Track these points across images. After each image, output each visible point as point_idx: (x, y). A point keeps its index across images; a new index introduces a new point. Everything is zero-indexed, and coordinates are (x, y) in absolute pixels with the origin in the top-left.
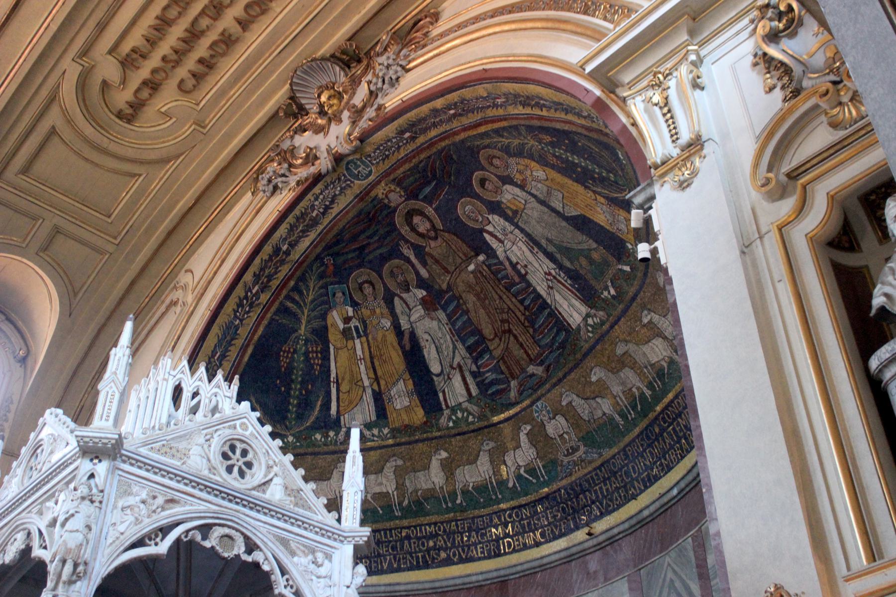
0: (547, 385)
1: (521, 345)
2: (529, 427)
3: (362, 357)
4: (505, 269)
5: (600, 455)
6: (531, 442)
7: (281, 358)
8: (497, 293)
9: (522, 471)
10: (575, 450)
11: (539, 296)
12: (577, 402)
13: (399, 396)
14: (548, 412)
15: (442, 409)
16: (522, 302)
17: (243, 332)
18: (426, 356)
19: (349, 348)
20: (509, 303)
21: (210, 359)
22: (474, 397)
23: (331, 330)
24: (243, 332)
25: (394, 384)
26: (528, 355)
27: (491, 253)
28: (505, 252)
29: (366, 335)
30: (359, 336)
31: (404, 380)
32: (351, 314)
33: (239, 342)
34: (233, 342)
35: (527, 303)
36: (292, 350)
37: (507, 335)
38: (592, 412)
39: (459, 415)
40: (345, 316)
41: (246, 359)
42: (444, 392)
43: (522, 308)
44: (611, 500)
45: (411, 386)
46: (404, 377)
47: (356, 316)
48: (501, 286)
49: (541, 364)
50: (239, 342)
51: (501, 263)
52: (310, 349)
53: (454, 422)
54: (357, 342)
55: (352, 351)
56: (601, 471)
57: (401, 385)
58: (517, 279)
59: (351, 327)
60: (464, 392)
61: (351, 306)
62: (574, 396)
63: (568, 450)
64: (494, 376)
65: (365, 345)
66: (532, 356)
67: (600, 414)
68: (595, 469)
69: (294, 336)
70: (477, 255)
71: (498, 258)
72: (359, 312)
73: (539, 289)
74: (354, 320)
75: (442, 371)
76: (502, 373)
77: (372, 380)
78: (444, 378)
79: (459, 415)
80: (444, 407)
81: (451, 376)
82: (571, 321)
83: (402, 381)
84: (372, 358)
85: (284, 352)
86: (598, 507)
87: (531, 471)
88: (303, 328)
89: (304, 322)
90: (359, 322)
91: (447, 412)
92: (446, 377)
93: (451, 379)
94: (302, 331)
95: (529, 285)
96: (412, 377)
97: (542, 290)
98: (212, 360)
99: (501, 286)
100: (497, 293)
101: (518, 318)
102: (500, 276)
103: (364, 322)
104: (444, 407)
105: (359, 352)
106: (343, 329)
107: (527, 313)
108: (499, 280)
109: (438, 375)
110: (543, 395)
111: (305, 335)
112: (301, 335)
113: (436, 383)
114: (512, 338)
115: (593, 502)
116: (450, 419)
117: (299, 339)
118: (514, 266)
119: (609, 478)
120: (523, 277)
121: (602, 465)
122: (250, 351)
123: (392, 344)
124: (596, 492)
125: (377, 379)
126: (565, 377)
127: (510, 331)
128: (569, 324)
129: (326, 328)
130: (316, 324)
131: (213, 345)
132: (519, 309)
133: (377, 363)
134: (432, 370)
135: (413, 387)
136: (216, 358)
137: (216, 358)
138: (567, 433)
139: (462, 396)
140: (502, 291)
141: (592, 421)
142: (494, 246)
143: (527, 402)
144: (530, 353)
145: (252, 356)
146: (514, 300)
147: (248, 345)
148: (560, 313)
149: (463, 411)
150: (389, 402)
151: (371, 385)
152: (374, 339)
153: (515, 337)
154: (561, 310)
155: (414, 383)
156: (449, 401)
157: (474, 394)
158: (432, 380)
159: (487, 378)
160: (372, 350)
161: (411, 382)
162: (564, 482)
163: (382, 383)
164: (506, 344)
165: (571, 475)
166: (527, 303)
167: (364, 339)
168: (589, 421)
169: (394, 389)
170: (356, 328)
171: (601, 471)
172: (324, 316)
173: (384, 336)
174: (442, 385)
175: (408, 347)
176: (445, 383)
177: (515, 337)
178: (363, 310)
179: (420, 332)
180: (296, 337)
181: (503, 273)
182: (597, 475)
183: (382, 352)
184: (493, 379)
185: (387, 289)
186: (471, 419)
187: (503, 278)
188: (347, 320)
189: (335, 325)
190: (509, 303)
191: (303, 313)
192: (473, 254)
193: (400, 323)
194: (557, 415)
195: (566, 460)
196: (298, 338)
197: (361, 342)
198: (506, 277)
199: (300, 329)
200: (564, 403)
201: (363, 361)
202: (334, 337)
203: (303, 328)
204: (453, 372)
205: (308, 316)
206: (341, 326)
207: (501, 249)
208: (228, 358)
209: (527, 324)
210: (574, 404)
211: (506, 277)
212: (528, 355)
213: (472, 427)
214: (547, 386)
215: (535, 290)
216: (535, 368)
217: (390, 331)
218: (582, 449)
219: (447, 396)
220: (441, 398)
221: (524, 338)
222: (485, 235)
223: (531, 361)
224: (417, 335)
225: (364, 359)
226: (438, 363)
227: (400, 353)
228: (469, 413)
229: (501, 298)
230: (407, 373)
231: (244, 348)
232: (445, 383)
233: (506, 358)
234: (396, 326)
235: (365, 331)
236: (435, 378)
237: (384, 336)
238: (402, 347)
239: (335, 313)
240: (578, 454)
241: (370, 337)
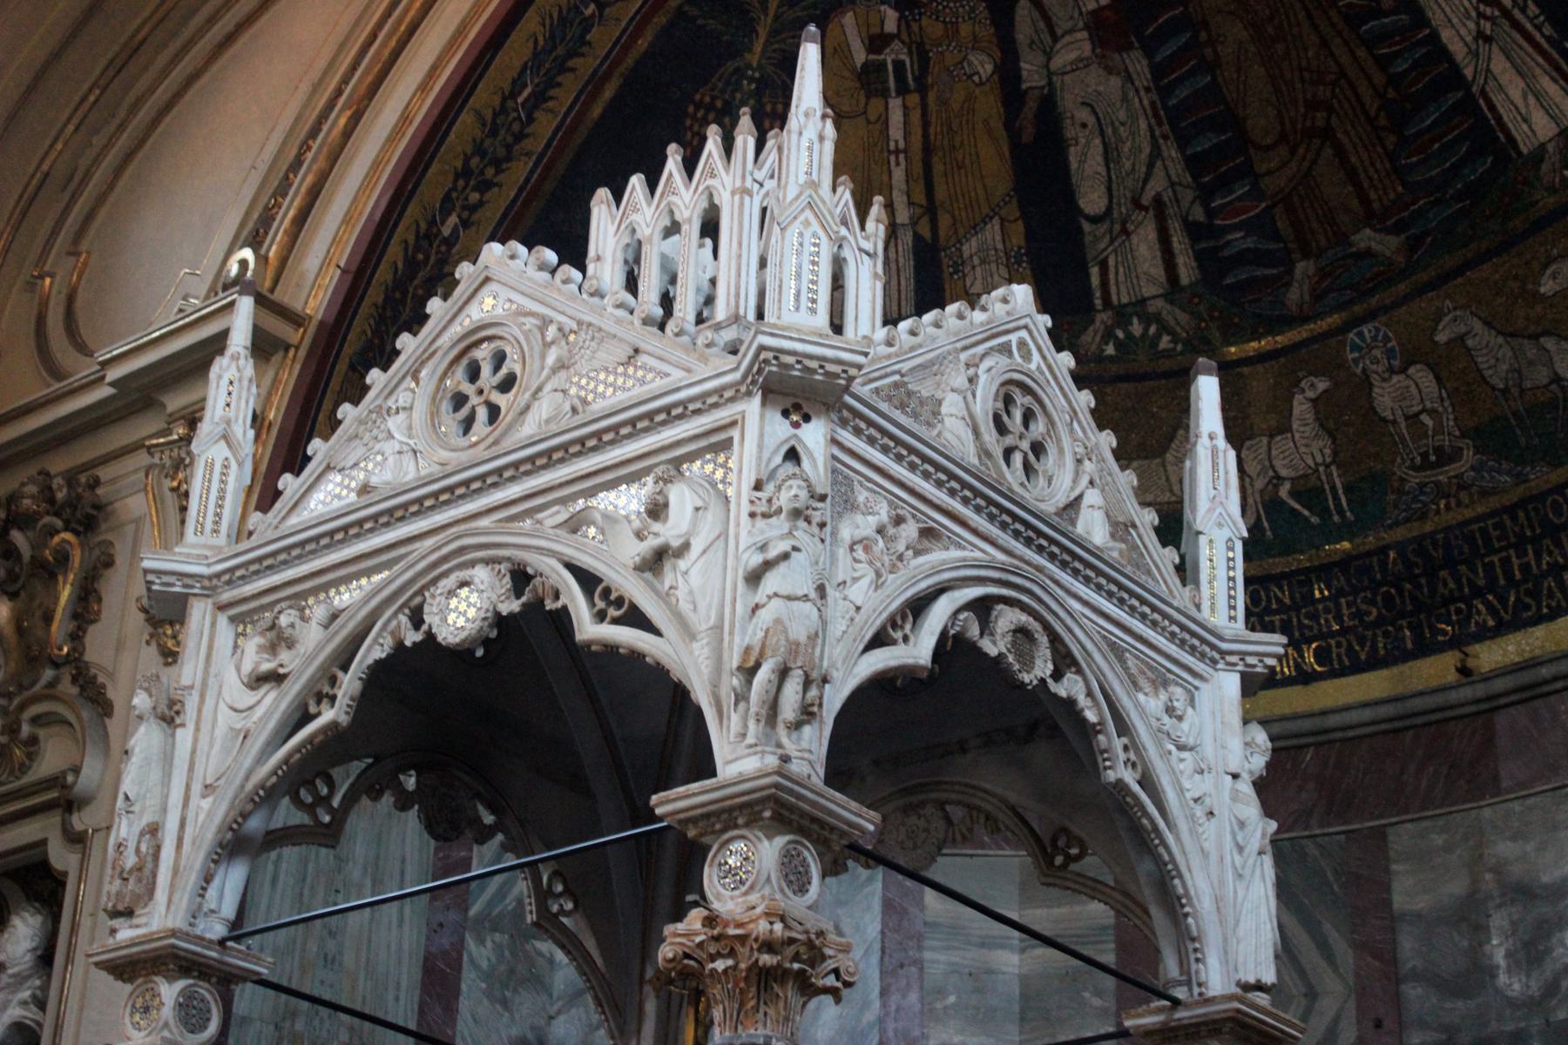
0: (1402, 286)
1: (1352, 176)
2: (1322, 385)
3: (902, 145)
5: (1521, 479)
6: (1321, 421)
7: (688, 122)
8: (1316, 27)
9: (1284, 492)
10: (1446, 457)
11: (1443, 53)
12: (1481, 337)
13: (983, 262)
14: (1390, 354)
15: (1091, 308)
16: (1383, 63)
17: (602, 38)
18: (1074, 165)
19: (872, 118)
20: (1345, 59)
21: (504, 100)
22: (1183, 289)
24: (602, 38)
25: (975, 228)
26: (1365, 201)
29: (923, 89)
30: (902, 90)
31: (1002, 220)
32: (891, 26)
33: (585, 65)
34: (570, 64)
35: (1401, 66)
36: (719, 104)
37: (1316, 142)
38: (1519, 372)
39: (1136, 328)
40: (875, 30)
41: (597, 111)
42: (1104, 265)
43: (1379, 79)
44: (1535, 594)
45: (1018, 238)
46: (1003, 212)
47: (905, 36)
48: (1333, 13)
49: (1397, 229)
50: (585, 65)
52: (768, 108)
53: (1119, 345)
54: (895, 104)
55: (878, 126)
56: (1514, 518)
57: (993, 232)
59: (883, 64)
60: (1159, 272)
61: (896, 8)
62: (1478, 326)
63: (1425, 456)
64: (1250, 243)
65: (916, 117)
66: (1376, 205)
67: (1542, 376)
68: (1493, 514)
69: (731, 66)
72: (915, 27)
73: (1446, 35)
74: (896, 45)
75: (1109, 209)
76: (1276, 236)
77: (919, 211)
78: (1111, 232)
79: (1136, 328)
80: (1098, 302)
81: (1131, 227)
82: (1519, 132)
83: (996, 221)
84: (928, 150)
85: (698, 106)
86: (1488, 605)
87: (1309, 492)
88: (758, 47)
89: (763, 33)
90: (910, 53)
91: (1102, 318)
92: (1117, 227)
93: (1128, 234)
94: (754, 58)
96: (1025, 216)
97: (1455, 41)
98: (510, 104)
99: (1333, 13)
100: (1316, 27)
101: (1362, 105)
104: (1098, 302)
105: (896, 133)
106: (865, 65)
107: (1391, 94)
109: (1095, 220)
110: (1386, 309)
111: (760, 67)
112: (749, 66)
113: (1088, 239)
114: (1328, 152)
115: (1478, 593)
116: (1108, 335)
117: (744, 76)
119: (1534, 540)
121: (1522, 503)
122: (608, 93)
124: (1489, 567)
125: (931, 209)
126: (1460, 271)
127: (1327, 133)
128: (1511, 140)
131: (518, 64)
132: (1369, 79)
133: (938, 168)
134: (1082, 203)
135: (1023, 243)
136: (520, 100)
137: (520, 100)
138: (1432, 413)
139: (1151, 280)
140: (1333, 25)
141: (1515, 391)
143: (1334, 320)
144: (1373, 195)
145: (614, 106)
146: (1362, 53)
147: (607, 76)
148: (1492, 108)
149: (1147, 319)
150: (956, 272)
151: (914, 222)
152: (943, 102)
153: (1340, 152)
154: (1497, 99)
155: (1030, 236)
156: (1113, 290)
157: (1185, 280)
158: (1080, 230)
159: (1229, 243)
160: (932, 131)
161: (1020, 227)
162: (1400, 534)
163: (944, 221)
164: (1306, 164)
165: (1423, 517)
166: (1401, 66)
167: (914, 99)
168: (1505, 391)
169: (974, 242)
170: (899, 66)
171: (1514, 518)
174: (1102, 246)
175: (1028, 135)
176: (1112, 241)
177: (1340, 152)
178: (925, 22)
179: (1068, 100)
180: (737, 70)
182: (1499, 526)
183: (958, 139)
184: (1248, 249)
186: (1165, 342)
188: (877, 42)
190: (1345, 59)
191: (765, 10)
193: (1019, 69)
194: (1414, 363)
195: (1414, 479)
197: (905, 107)
199: (750, 50)
200: (1441, 337)
201: (902, 157)
203: (758, 47)
204: (1138, 216)
205: (777, 17)
206: (860, 56)
208: (551, 104)
209: (1382, 121)
210: (1470, 343)
212: (1365, 201)
213: (1166, 365)
214: (1402, 288)
215: (1434, 37)
216: (1378, 236)
217: (987, 87)
218: (1469, 456)
219: (1112, 276)
220: (1095, 280)
221: (1365, 156)
223: (1370, 217)
224: (1061, 109)
225: (905, 151)
226: (1103, 189)
227: (1006, 150)
228: (1164, 328)
229: (1324, 44)
230: (1015, 201)
231: (596, 82)
232: (1112, 241)
233: (1295, 199)
234: (1008, 74)
235: (920, 80)
236: (1086, 226)
239: (849, 19)
240: (1452, 469)
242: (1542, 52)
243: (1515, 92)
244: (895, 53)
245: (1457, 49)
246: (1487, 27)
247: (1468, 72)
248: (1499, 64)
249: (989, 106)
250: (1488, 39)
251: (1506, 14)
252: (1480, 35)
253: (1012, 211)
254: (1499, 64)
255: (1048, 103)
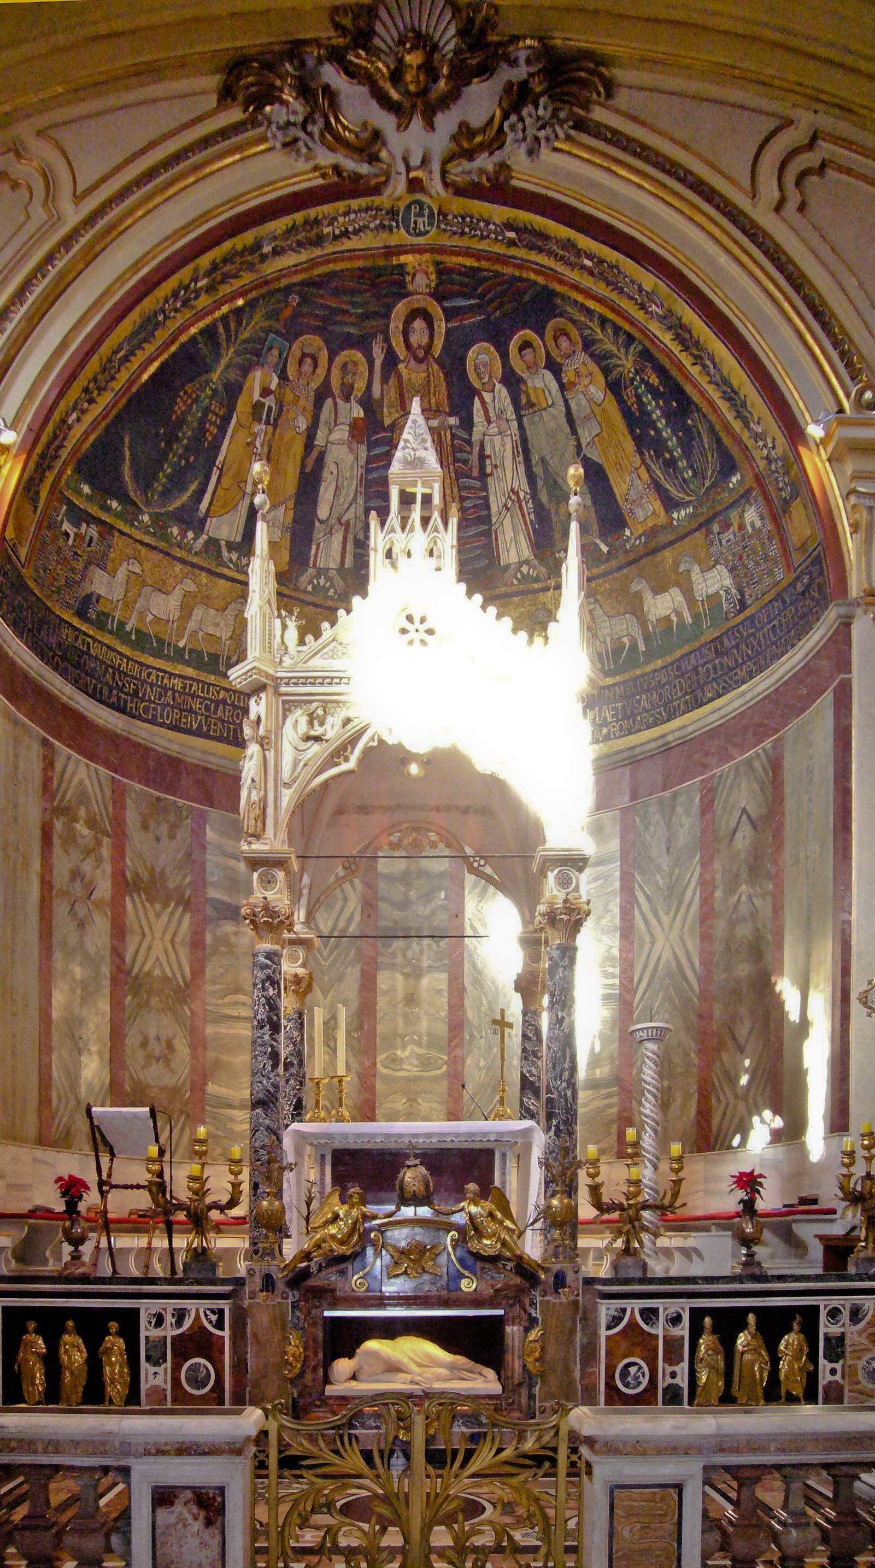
4: (470, 453)
11: (488, 507)
23: (245, 394)
27: (467, 423)
28: (484, 435)
29: (275, 427)
30: (267, 423)
51: (469, 442)
58: (475, 473)
70: (451, 415)
71: (470, 435)
73: (492, 499)
88: (218, 372)
94: (215, 377)
95: (485, 488)
102: (458, 455)
103: (281, 407)
106: (258, 401)
108: (456, 460)
118: (483, 457)
120: (483, 476)
123: (294, 455)
129: (241, 389)
130: (233, 376)
142: (476, 419)
152: (281, 435)
170: (270, 408)
172: (246, 370)
173: (293, 438)
175: (308, 470)
179: (329, 460)
181: (464, 455)
185: (326, 383)
187: (459, 461)
189: (251, 389)
192: (447, 410)
196: (207, 382)
198: (465, 462)
199: (215, 371)
202: (243, 406)
203: (218, 372)
206: (256, 396)
207: (481, 428)
211: (465, 462)
215: (486, 498)
222: (477, 400)
237: (293, 438)
238: (303, 465)
241: (278, 430)
242: (526, 524)
243: (508, 538)
244: (269, 401)
245: (494, 508)
246: (510, 504)
247: (494, 520)
248: (507, 522)
249: (298, 448)
250: (508, 509)
251: (519, 501)
252: (505, 506)
253: (291, 504)
254: (507, 522)
255: (321, 460)
